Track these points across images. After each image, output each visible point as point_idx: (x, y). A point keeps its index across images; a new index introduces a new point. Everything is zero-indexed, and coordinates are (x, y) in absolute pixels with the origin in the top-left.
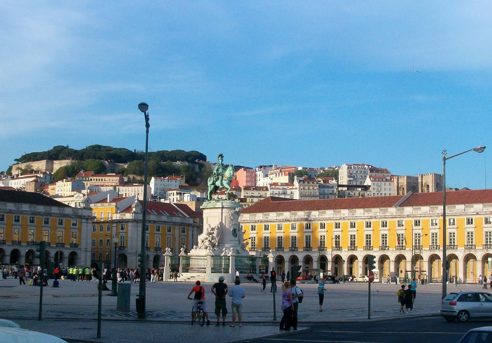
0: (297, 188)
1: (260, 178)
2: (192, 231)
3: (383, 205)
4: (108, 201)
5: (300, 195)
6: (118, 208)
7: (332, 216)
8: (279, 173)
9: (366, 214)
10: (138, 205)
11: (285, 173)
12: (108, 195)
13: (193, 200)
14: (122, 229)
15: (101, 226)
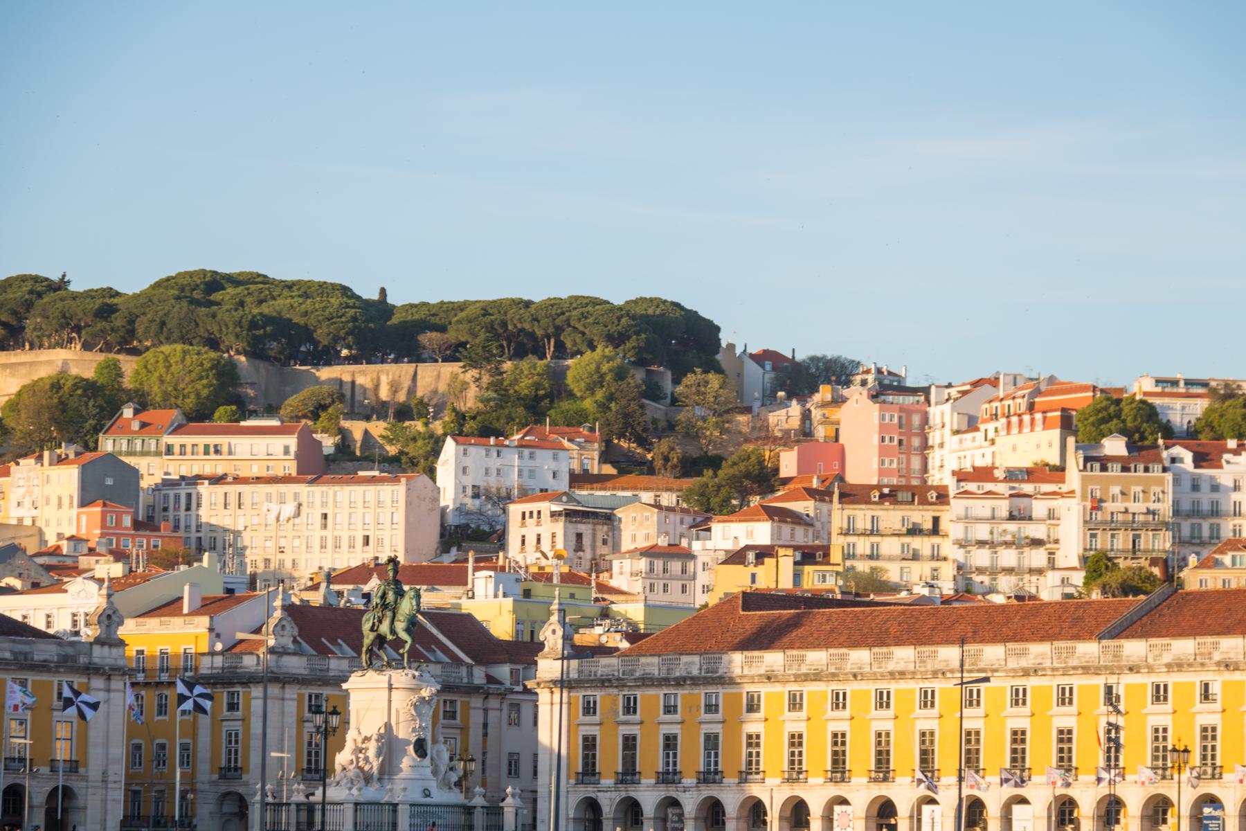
0: (1073, 492)
1: (942, 436)
2: (481, 713)
3: (1074, 631)
4: (186, 611)
5: (1085, 522)
6: (218, 636)
7: (911, 667)
8: (1020, 415)
9: (1013, 663)
10: (283, 627)
11: (1045, 419)
12: (186, 588)
13: (505, 595)
14: (232, 707)
15: (160, 696)
